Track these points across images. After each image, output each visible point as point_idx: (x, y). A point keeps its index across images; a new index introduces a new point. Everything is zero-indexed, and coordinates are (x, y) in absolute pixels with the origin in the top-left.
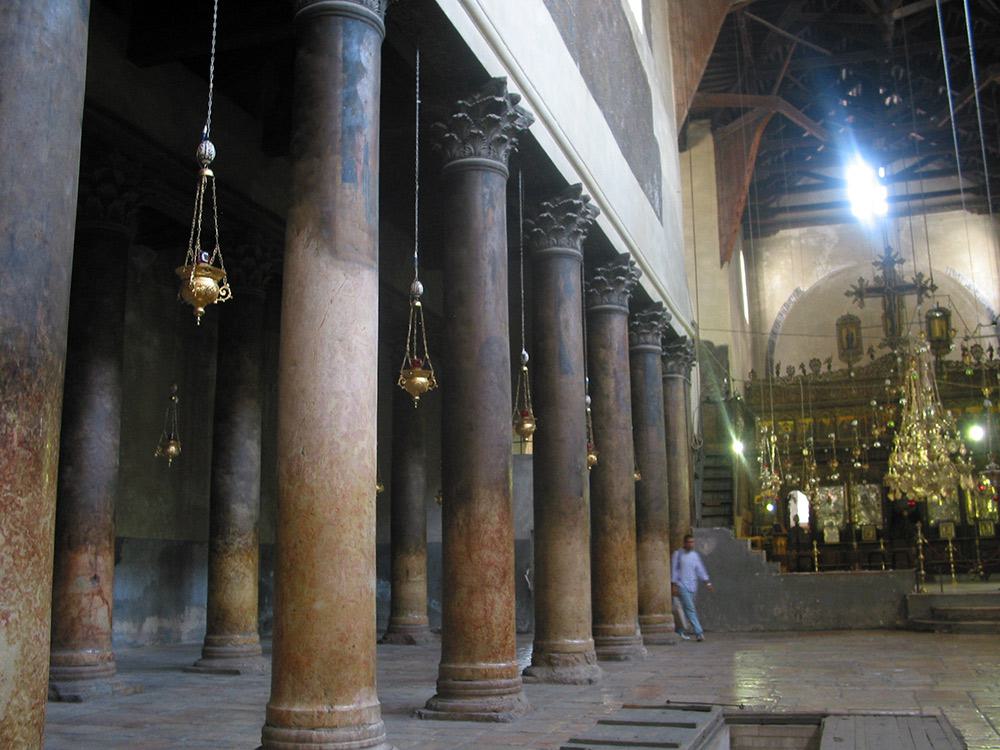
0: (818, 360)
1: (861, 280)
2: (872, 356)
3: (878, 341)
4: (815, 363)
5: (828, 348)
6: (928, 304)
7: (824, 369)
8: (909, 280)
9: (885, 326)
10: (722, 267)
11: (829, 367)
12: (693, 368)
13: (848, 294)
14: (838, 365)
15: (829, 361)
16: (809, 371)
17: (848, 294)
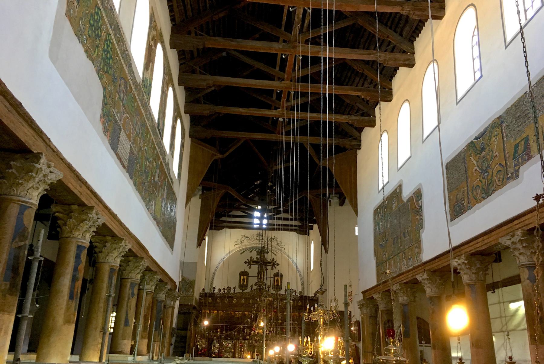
0: (230, 287)
1: (251, 258)
2: (252, 289)
3: (254, 283)
4: (229, 288)
5: (234, 283)
6: (275, 271)
7: (232, 291)
8: (269, 260)
9: (258, 277)
10: (197, 248)
11: (234, 291)
12: (177, 301)
13: (245, 262)
14: (238, 290)
15: (234, 288)
16: (226, 291)
17: (245, 262)
